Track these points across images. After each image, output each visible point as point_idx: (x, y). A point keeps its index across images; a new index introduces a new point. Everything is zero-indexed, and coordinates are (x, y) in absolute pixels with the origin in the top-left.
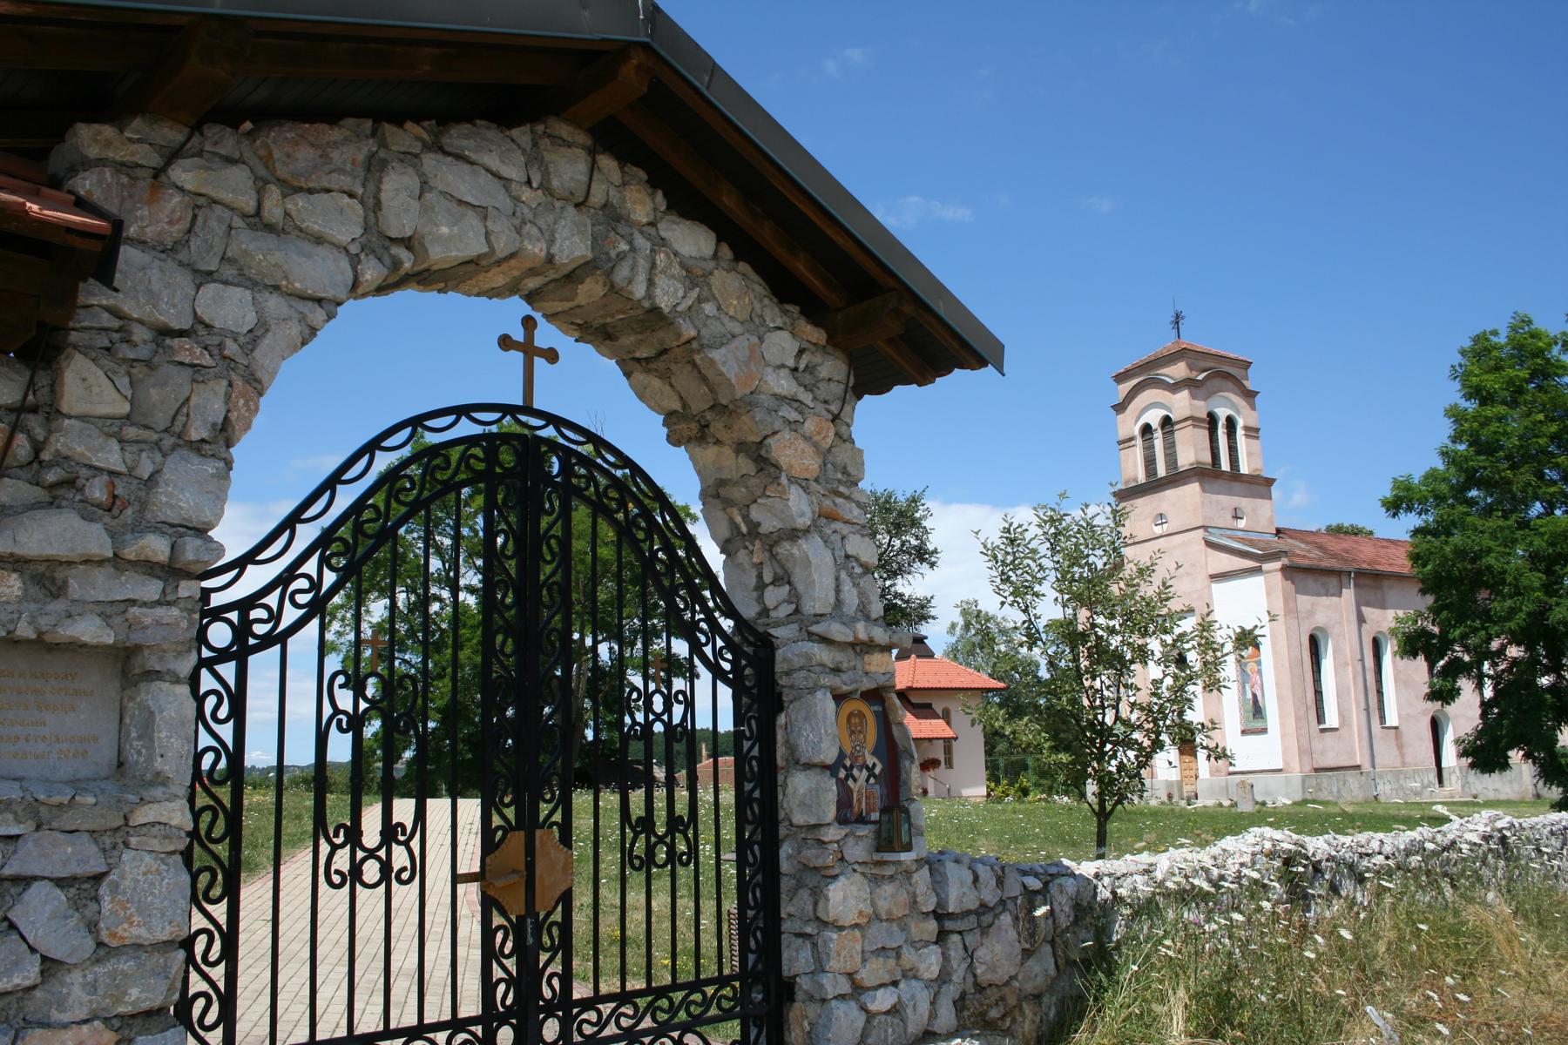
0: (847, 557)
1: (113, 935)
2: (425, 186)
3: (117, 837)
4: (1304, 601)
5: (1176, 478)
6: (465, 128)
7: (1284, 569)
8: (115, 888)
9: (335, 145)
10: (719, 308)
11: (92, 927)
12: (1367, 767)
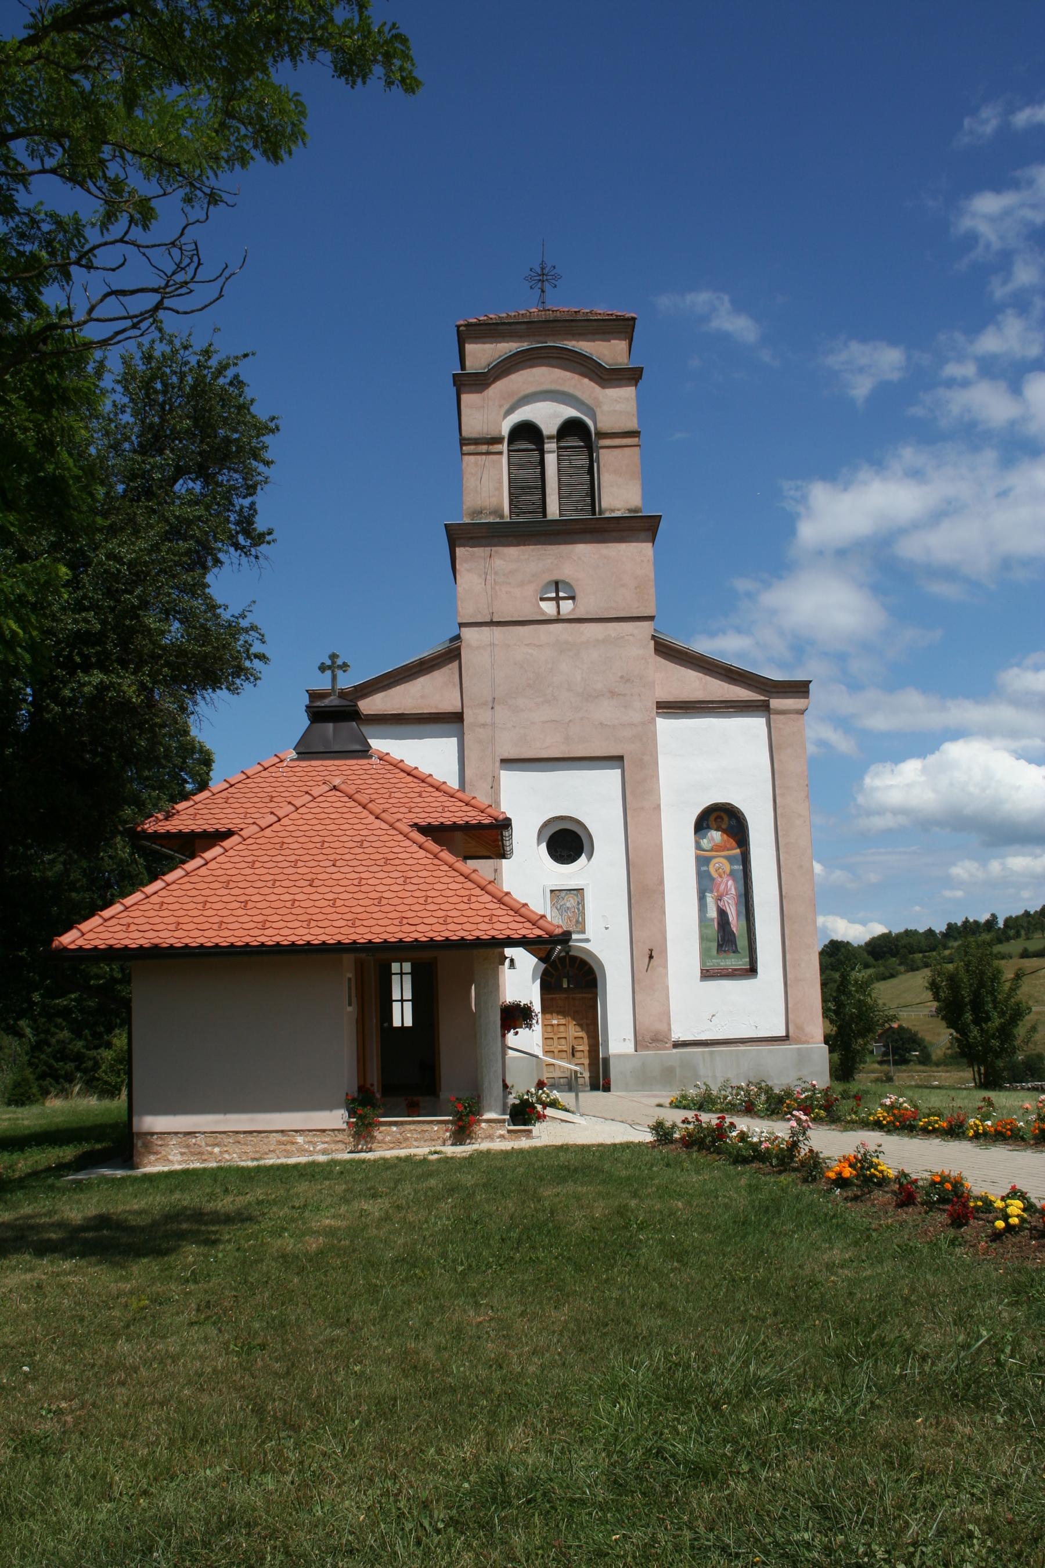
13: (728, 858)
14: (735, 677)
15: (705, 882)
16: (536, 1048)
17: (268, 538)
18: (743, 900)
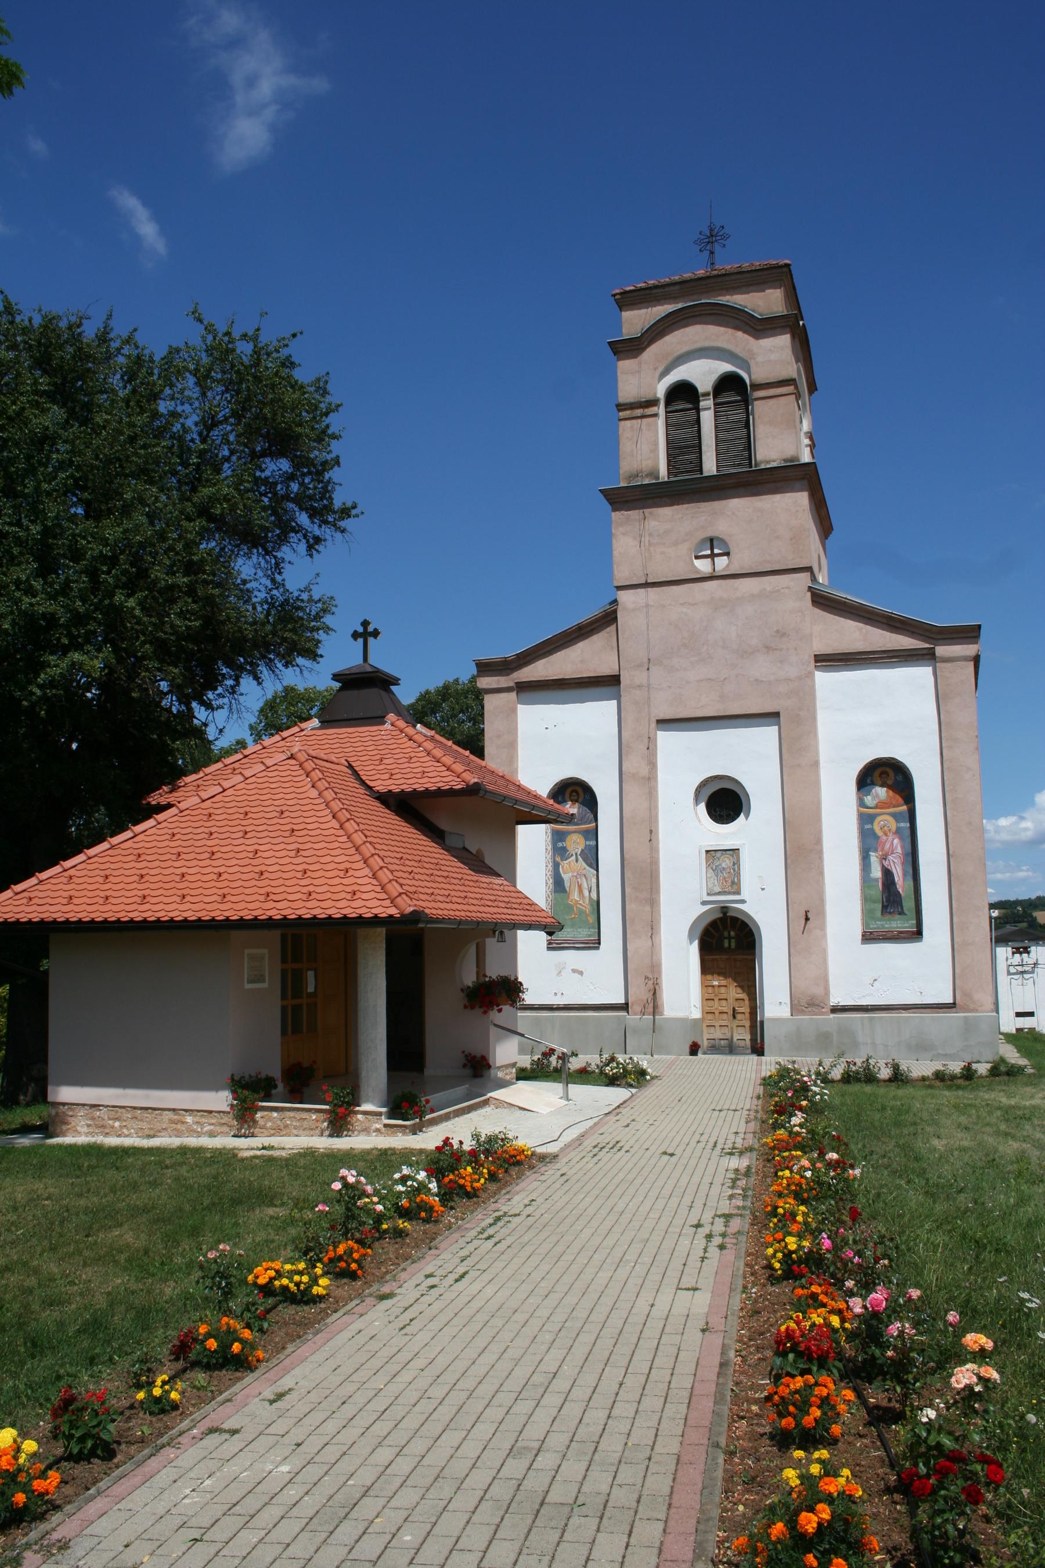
13: (894, 815)
14: (897, 625)
15: (868, 841)
16: (693, 1008)
17: (354, 512)
18: (910, 859)
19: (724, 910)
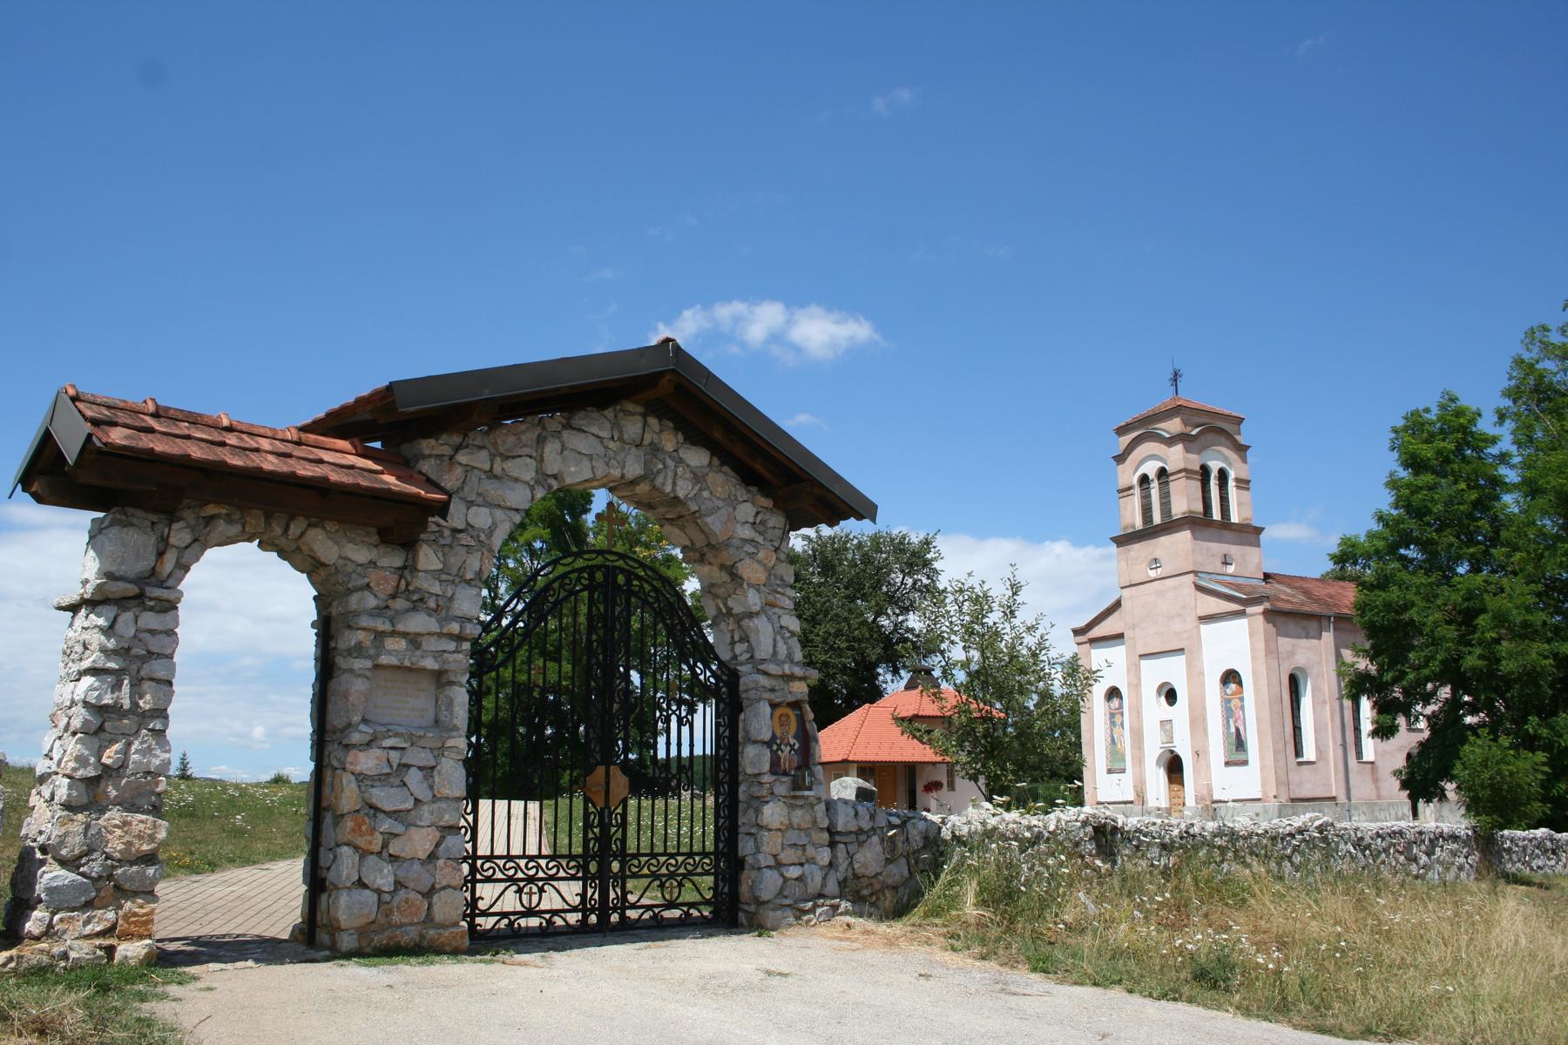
0: (781, 627)
1: (439, 792)
2: (564, 448)
3: (440, 751)
4: (1285, 643)
5: (1170, 526)
6: (582, 414)
7: (1266, 613)
8: (439, 772)
9: (523, 432)
10: (711, 493)
11: (431, 787)
12: (1342, 798)
15: (1228, 713)
19: (1172, 752)
